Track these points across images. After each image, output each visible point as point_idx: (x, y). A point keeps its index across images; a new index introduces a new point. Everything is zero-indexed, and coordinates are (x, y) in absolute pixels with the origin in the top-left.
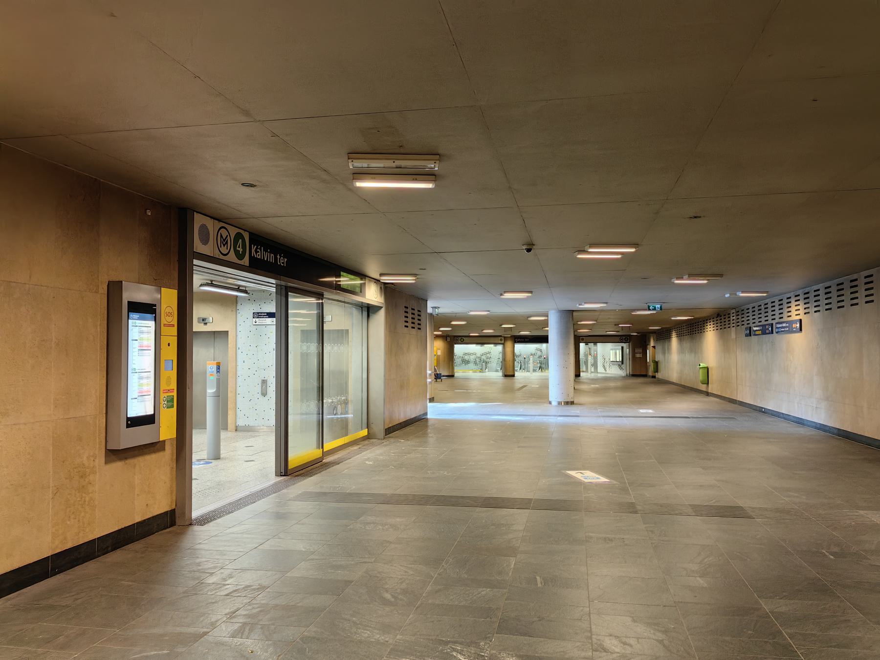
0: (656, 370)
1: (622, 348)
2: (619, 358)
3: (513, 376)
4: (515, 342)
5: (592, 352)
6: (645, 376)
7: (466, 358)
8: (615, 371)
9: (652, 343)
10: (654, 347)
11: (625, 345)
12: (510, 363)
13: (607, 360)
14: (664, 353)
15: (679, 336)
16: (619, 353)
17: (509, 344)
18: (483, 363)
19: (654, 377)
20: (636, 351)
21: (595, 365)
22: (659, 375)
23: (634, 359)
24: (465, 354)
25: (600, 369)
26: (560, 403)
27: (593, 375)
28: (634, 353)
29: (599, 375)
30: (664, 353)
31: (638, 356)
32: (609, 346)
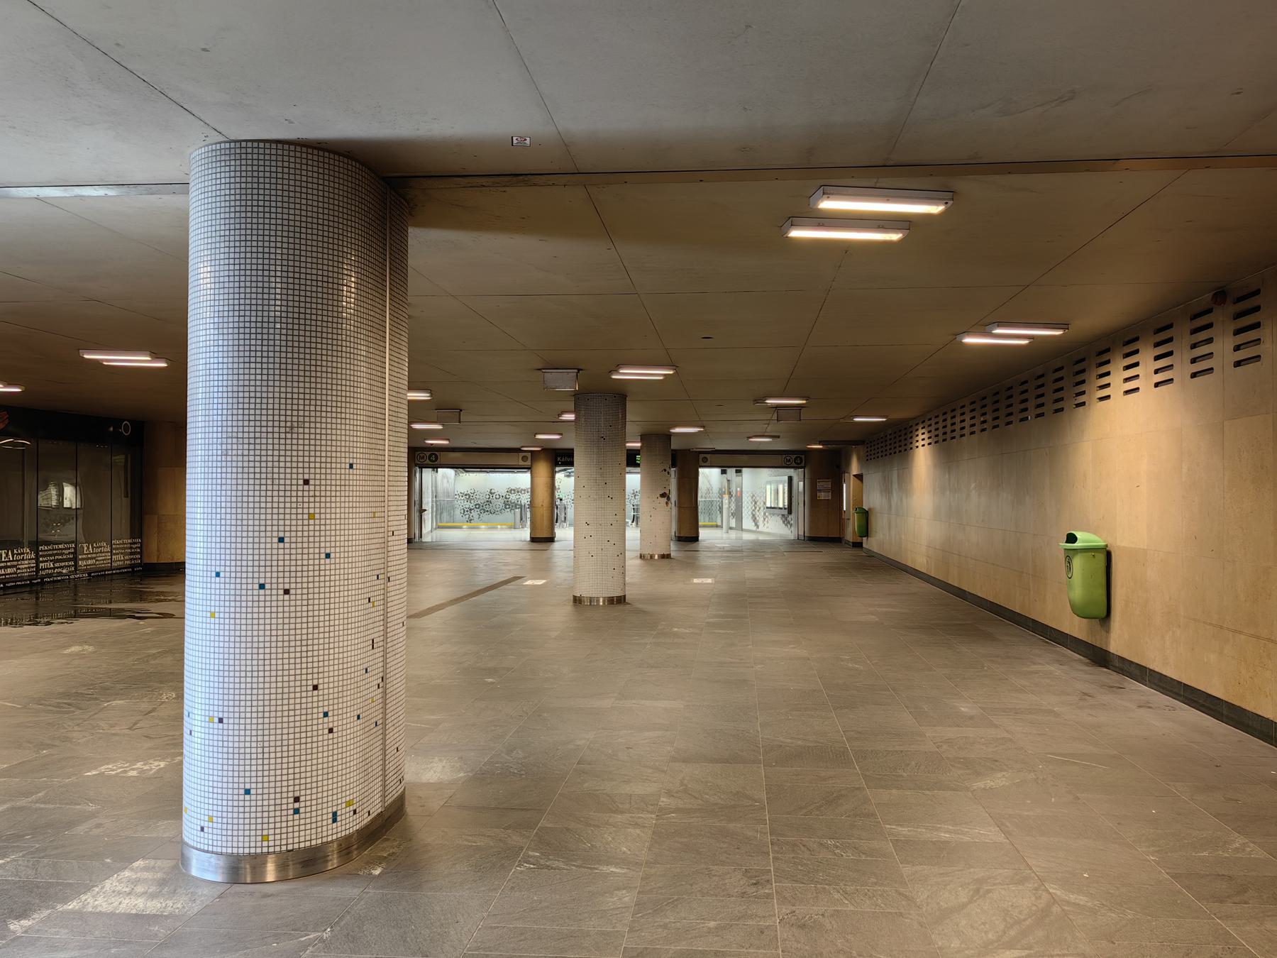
0: (866, 531)
1: (790, 479)
2: (782, 502)
3: (551, 540)
4: (557, 464)
5: (733, 489)
6: (837, 540)
7: (513, 497)
8: (774, 529)
9: (855, 468)
10: (859, 477)
11: (796, 474)
12: (543, 512)
13: (760, 504)
14: (887, 490)
15: (944, 441)
16: (783, 489)
17: (542, 468)
18: (484, 507)
19: (858, 545)
20: (820, 485)
21: (738, 514)
22: (872, 544)
23: (814, 502)
24: (511, 491)
25: (748, 523)
26: (241, 869)
27: (733, 534)
28: (813, 490)
29: (747, 537)
30: (887, 490)
31: (822, 496)
32: (765, 474)
